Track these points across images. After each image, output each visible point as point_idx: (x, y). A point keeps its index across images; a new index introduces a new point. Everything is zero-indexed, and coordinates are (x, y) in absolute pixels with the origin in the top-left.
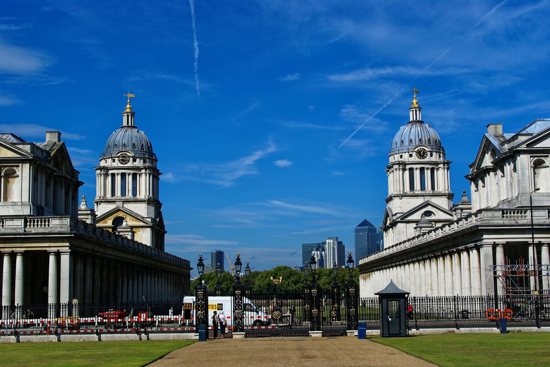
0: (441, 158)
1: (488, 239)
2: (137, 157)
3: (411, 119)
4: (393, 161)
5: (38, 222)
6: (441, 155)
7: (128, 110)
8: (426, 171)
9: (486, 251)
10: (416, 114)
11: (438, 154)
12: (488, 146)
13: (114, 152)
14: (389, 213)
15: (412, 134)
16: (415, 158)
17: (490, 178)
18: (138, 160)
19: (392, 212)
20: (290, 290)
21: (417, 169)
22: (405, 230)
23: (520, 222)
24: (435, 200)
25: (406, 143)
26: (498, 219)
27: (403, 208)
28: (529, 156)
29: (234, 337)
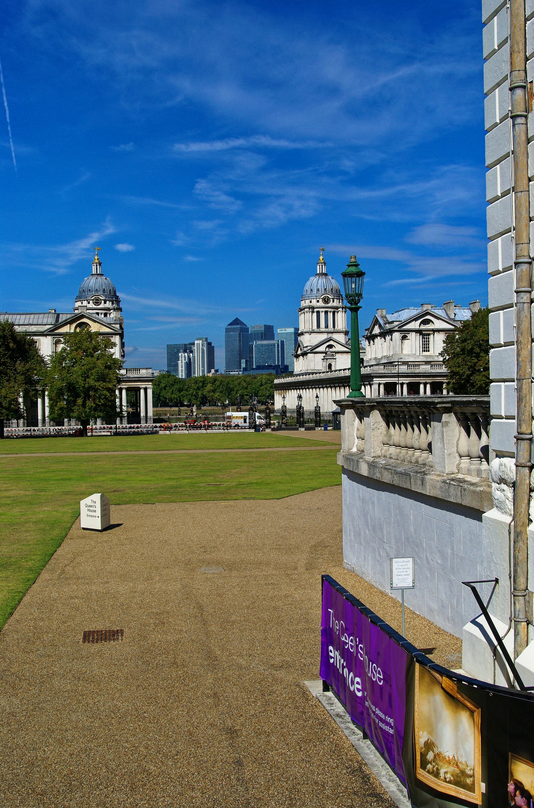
0: (341, 303)
1: (376, 381)
2: (107, 300)
3: (318, 272)
4: (304, 305)
5: (133, 371)
6: (341, 301)
7: (96, 261)
8: (329, 313)
9: (375, 387)
10: (322, 268)
11: (338, 300)
12: (376, 322)
13: (89, 296)
14: (301, 345)
15: (319, 285)
16: (321, 304)
17: (378, 340)
18: (108, 302)
19: (303, 345)
20: (174, 398)
21: (322, 312)
22: (313, 359)
23: (393, 372)
24: (335, 336)
25: (315, 291)
26: (381, 370)
27: (312, 342)
28: (399, 333)
29: (266, 431)
